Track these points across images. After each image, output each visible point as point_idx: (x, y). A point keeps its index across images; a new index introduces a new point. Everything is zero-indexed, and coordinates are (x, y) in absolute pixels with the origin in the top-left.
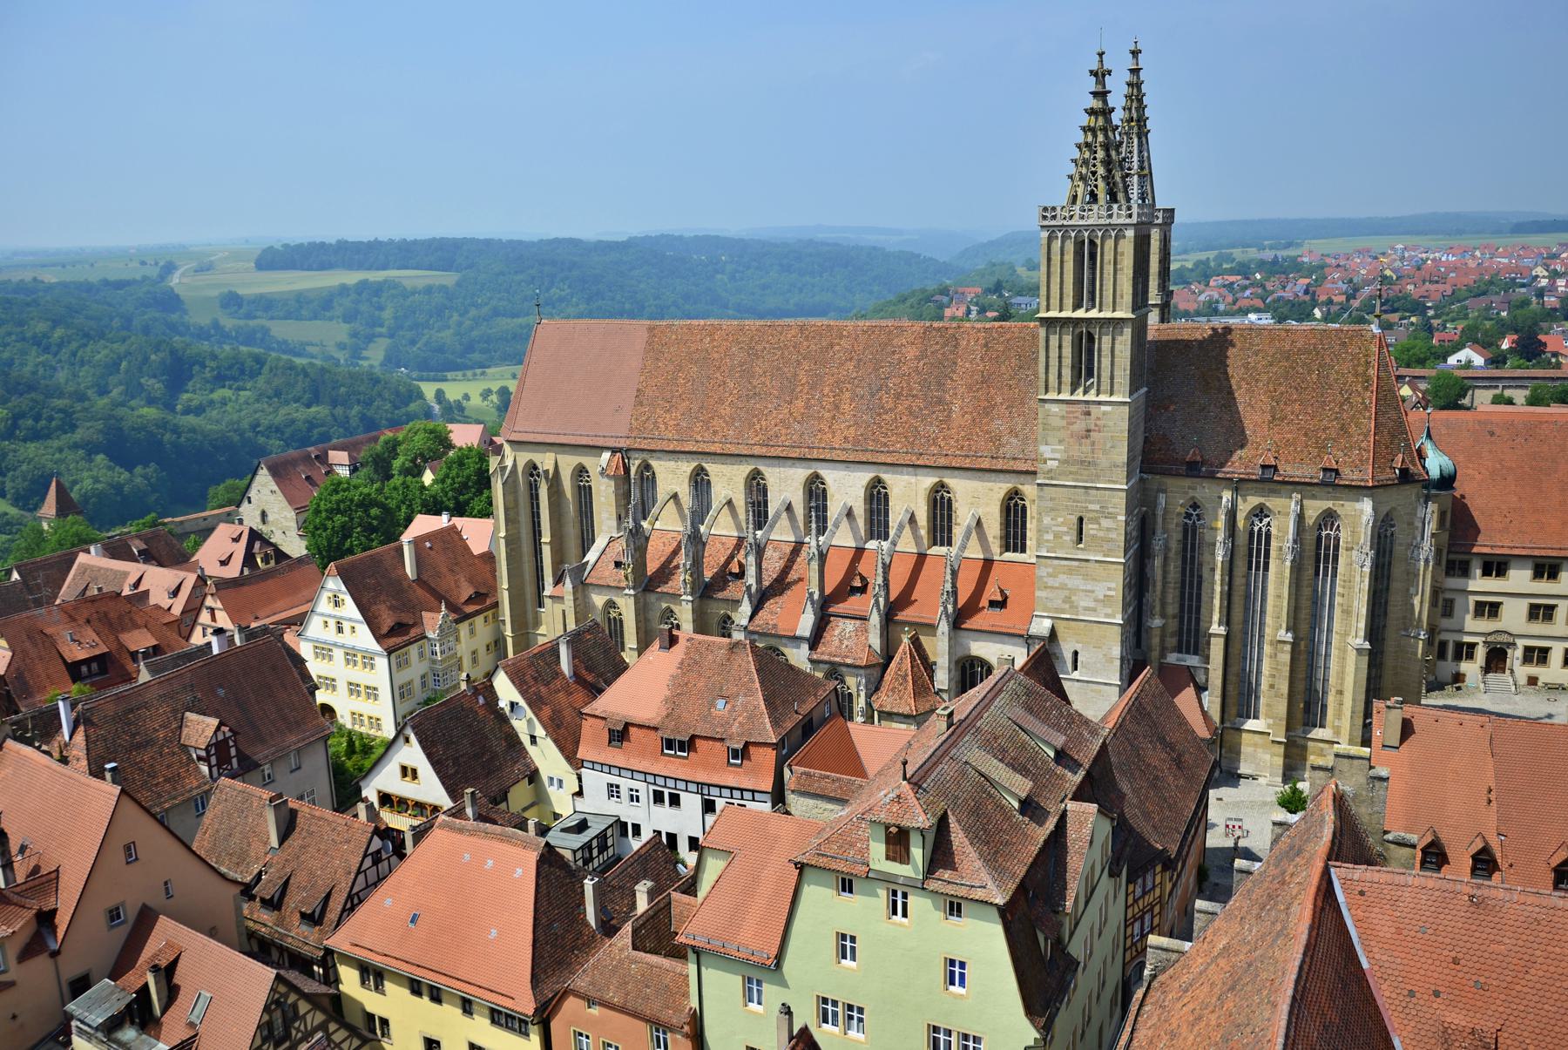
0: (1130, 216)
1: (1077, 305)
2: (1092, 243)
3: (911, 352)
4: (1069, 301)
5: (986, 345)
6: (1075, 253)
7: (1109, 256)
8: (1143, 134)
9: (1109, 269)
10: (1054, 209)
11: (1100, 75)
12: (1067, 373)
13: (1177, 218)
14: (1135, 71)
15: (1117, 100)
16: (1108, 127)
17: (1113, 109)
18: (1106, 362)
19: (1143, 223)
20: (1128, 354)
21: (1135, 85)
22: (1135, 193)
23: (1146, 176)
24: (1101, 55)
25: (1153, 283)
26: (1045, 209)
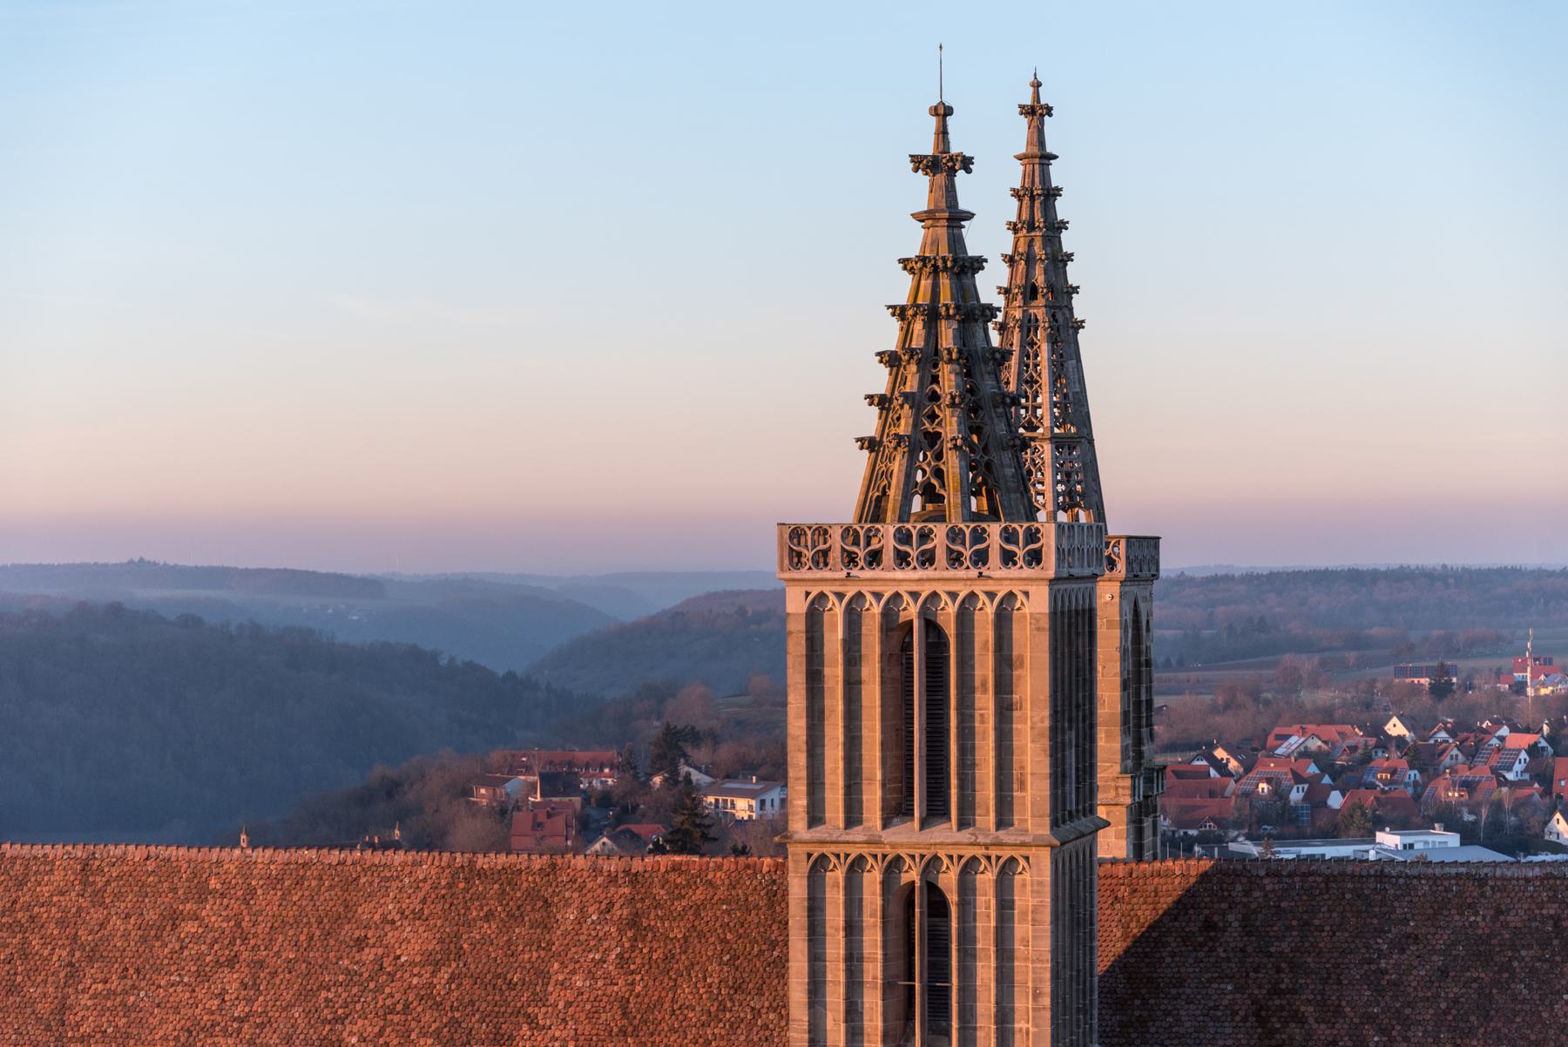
0: (1035, 558)
1: (897, 810)
2: (931, 626)
3: (412, 942)
4: (873, 797)
5: (634, 922)
6: (886, 658)
7: (985, 667)
8: (1065, 331)
9: (985, 703)
10: (822, 531)
11: (942, 165)
12: (873, 1003)
13: (1170, 562)
14: (1039, 158)
15: (990, 236)
16: (973, 314)
17: (978, 264)
18: (985, 971)
19: (1071, 578)
20: (1046, 945)
21: (1039, 199)
22: (1046, 489)
23: (1076, 438)
24: (943, 112)
25: (1109, 745)
26: (797, 533)
